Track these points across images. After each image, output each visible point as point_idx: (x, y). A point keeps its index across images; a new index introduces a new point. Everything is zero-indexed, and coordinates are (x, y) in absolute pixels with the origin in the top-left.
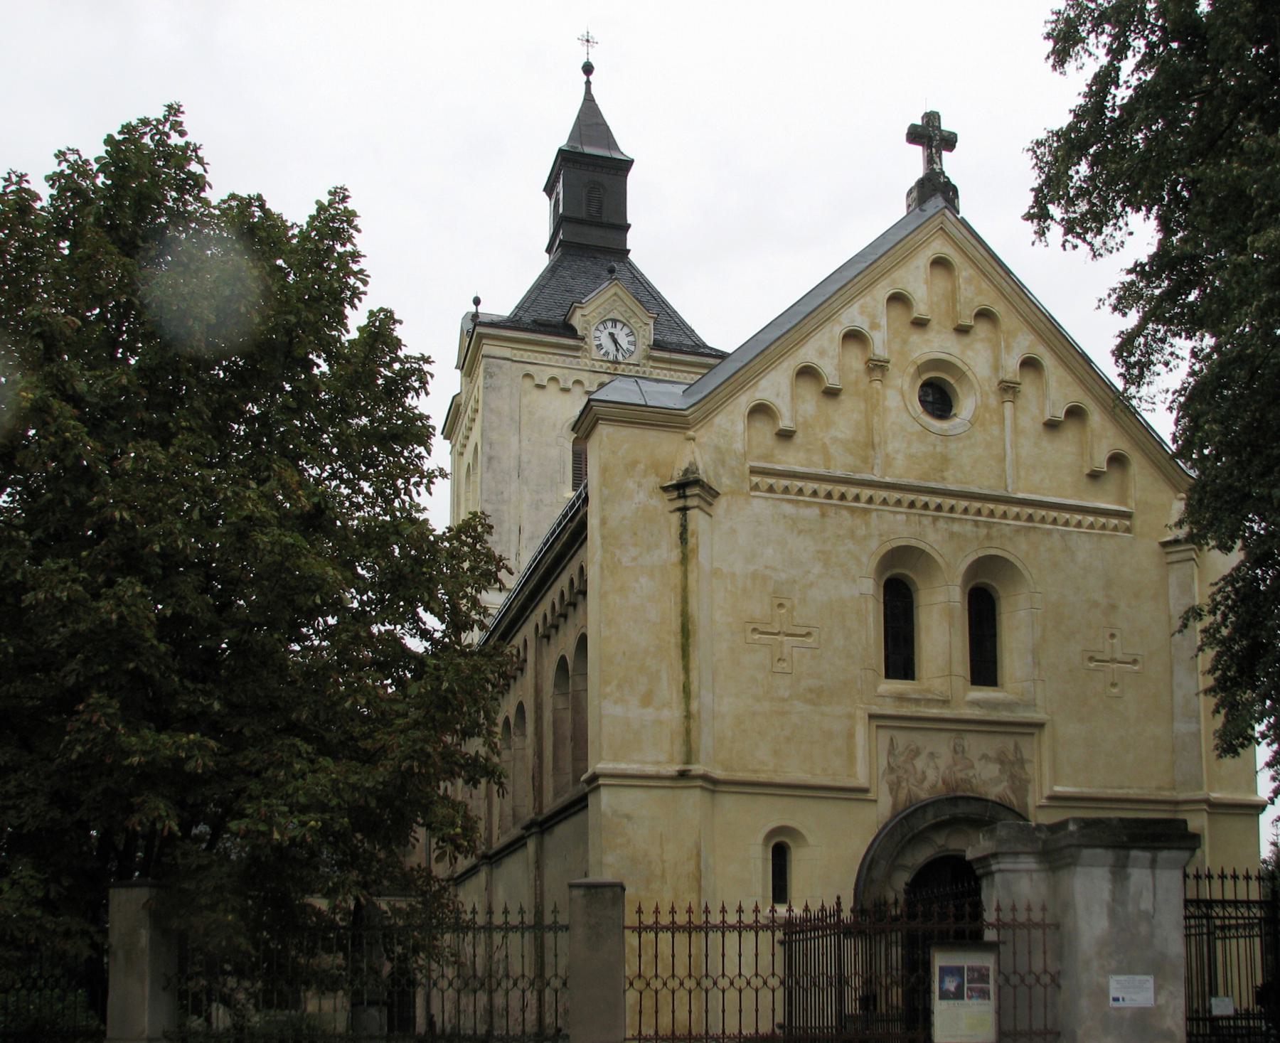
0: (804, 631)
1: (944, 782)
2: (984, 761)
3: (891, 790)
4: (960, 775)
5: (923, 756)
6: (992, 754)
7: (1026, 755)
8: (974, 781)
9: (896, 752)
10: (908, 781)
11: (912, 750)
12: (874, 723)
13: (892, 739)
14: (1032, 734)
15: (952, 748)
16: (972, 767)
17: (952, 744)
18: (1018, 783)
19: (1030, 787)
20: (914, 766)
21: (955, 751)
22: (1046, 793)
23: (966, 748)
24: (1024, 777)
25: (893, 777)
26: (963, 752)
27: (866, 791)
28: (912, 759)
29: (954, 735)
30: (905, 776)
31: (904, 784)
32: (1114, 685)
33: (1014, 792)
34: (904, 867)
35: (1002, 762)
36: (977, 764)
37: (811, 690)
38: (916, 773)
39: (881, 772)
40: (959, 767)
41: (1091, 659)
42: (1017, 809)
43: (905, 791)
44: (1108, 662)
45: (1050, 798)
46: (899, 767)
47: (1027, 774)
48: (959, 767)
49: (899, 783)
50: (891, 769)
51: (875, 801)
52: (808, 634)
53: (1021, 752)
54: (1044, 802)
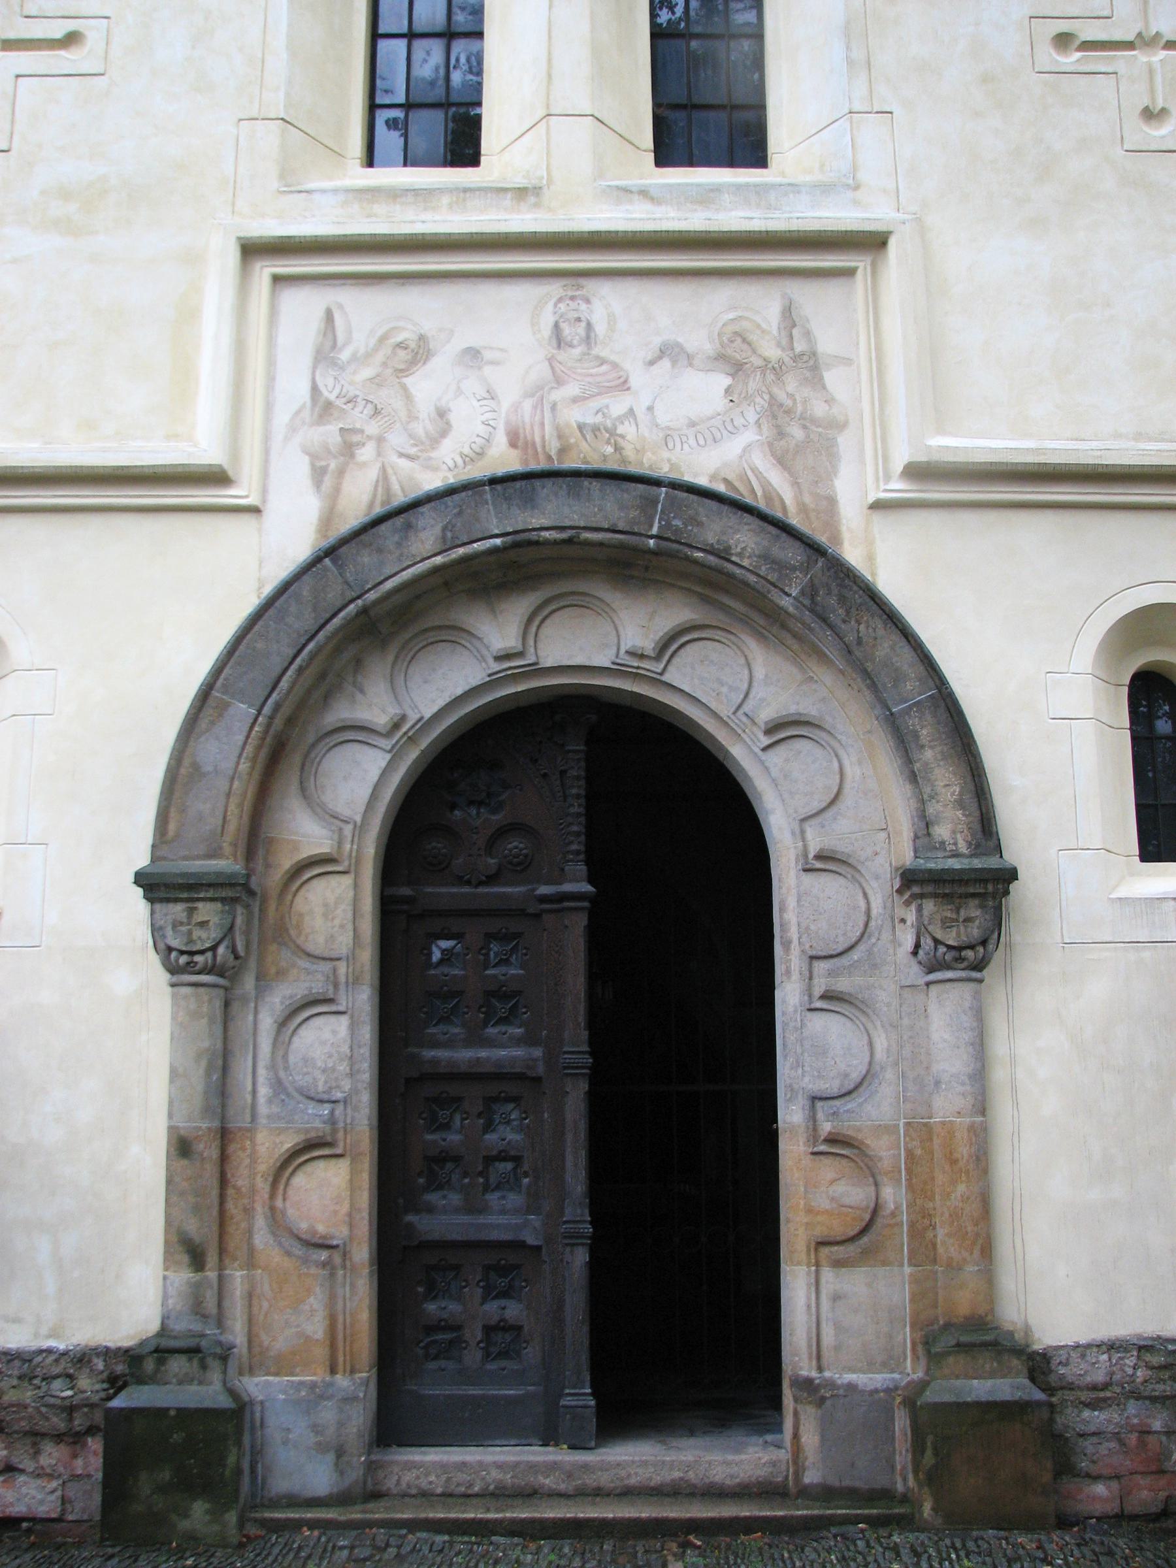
0: (57, 30)
1: (514, 439)
2: (666, 363)
3: (318, 474)
4: (574, 416)
5: (441, 365)
6: (699, 341)
7: (827, 344)
8: (627, 429)
9: (345, 355)
10: (380, 440)
11: (401, 345)
12: (265, 270)
13: (329, 317)
14: (850, 273)
15: (546, 330)
16: (624, 386)
17: (547, 319)
18: (797, 433)
19: (845, 442)
20: (408, 396)
21: (559, 339)
22: (900, 458)
23: (600, 329)
24: (819, 409)
25: (330, 433)
26: (589, 337)
27: (217, 477)
28: (401, 372)
29: (555, 288)
30: (372, 428)
31: (366, 453)
32: (1150, 115)
33: (782, 461)
34: (360, 731)
35: (737, 368)
36: (638, 377)
37: (65, 194)
38: (412, 417)
39: (282, 418)
40: (572, 389)
41: (1063, 41)
42: (794, 521)
43: (373, 474)
44: (1129, 45)
45: (917, 472)
46: (351, 401)
47: (830, 401)
48: (572, 389)
49: (348, 449)
50: (323, 409)
51: (255, 510)
52: (71, 39)
53: (808, 334)
54: (898, 488)
